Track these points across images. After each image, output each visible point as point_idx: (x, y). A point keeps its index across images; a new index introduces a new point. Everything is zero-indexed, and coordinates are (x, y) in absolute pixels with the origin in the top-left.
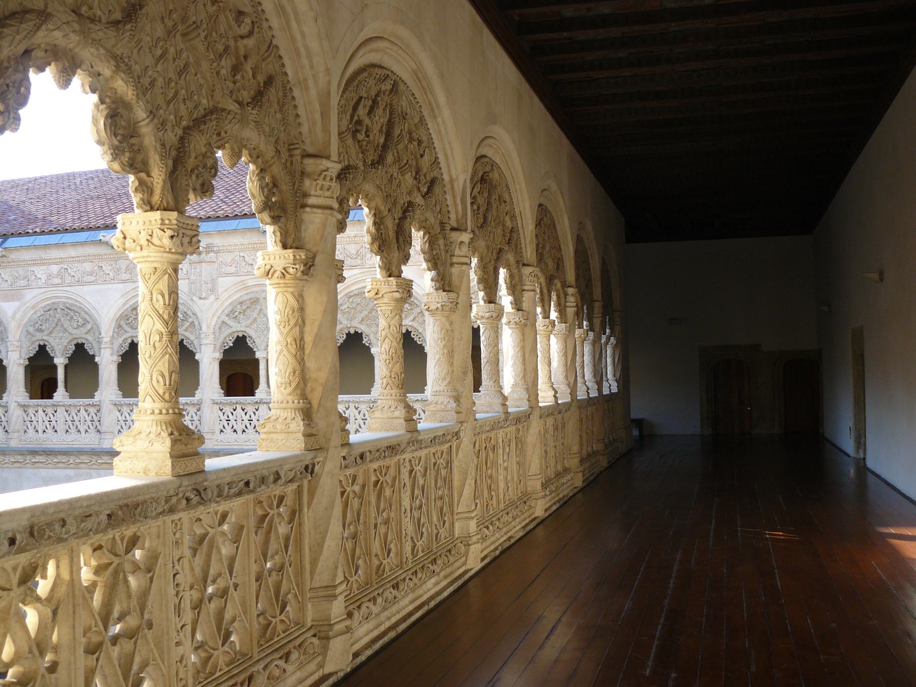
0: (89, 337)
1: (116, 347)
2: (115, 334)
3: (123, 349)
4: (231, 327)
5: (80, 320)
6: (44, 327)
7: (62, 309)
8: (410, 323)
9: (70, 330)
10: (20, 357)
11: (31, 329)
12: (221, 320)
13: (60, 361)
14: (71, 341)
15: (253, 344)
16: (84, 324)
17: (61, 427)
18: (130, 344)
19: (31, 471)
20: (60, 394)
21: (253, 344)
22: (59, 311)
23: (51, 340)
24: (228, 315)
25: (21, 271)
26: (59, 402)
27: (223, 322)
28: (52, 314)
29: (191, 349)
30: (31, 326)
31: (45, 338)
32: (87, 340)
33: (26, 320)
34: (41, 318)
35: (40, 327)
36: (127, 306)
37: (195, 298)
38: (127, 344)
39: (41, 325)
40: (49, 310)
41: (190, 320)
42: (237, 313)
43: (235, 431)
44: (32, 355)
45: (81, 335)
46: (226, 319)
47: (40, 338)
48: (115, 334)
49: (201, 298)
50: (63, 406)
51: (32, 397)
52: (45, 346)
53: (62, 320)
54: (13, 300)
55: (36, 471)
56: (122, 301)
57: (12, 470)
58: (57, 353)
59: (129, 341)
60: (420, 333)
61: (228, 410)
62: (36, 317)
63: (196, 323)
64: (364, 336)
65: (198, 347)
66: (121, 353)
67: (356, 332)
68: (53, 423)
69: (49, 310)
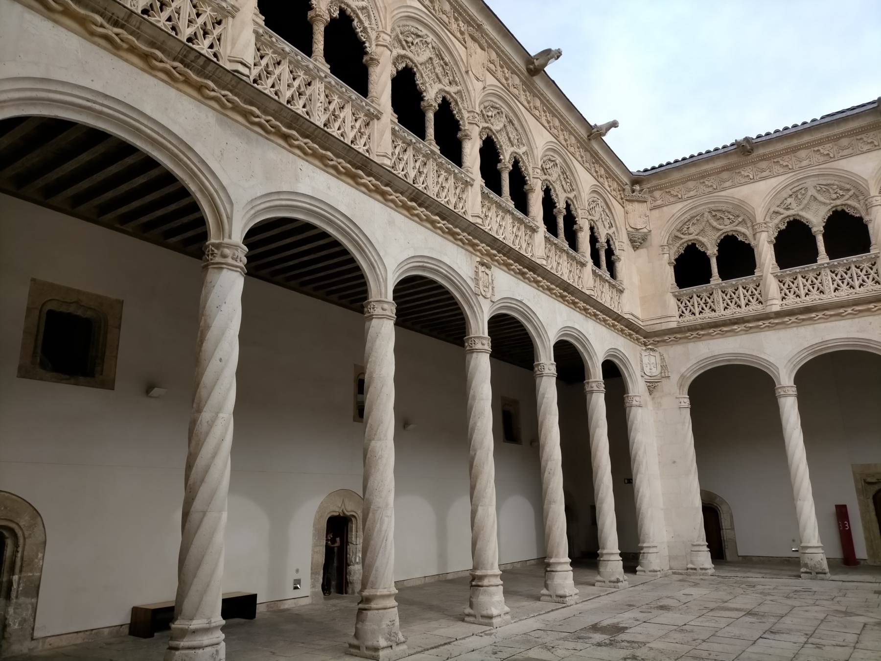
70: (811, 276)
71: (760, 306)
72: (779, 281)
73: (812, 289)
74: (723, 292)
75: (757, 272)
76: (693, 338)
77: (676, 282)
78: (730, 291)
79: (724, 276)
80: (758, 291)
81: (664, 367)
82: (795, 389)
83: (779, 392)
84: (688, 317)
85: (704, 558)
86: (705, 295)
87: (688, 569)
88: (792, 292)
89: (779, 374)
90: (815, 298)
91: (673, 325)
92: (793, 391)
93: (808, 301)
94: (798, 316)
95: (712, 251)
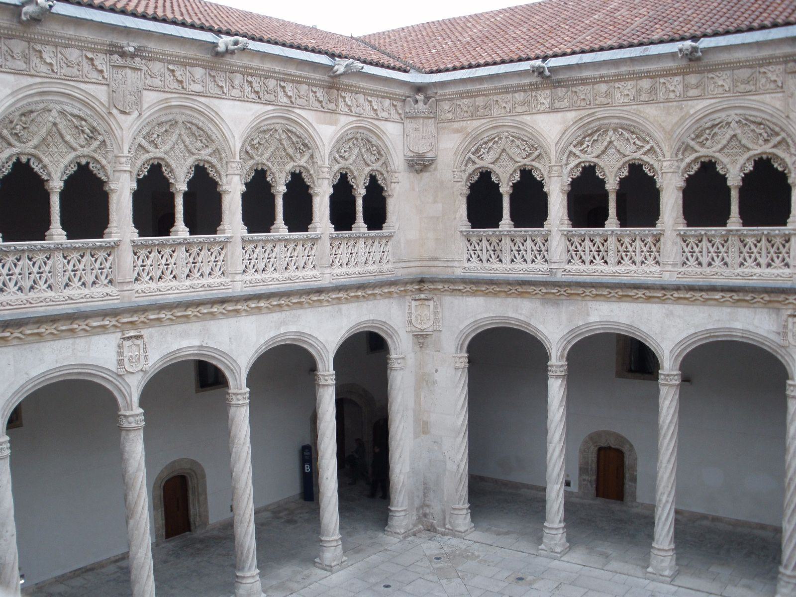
3: (4, 170)
4: (148, 152)
8: (305, 165)
12: (137, 142)
15: (170, 175)
18: (14, 164)
21: (170, 175)
24: (144, 138)
27: (140, 145)
29: (99, 176)
36: (13, 109)
37: (114, 111)
38: (10, 163)
41: (100, 138)
42: (155, 136)
43: (481, 260)
46: (144, 143)
49: (123, 112)
51: (575, 225)
60: (310, 175)
61: (576, 240)
63: (108, 143)
64: (268, 173)
65: (112, 174)
67: (262, 169)
68: (498, 252)
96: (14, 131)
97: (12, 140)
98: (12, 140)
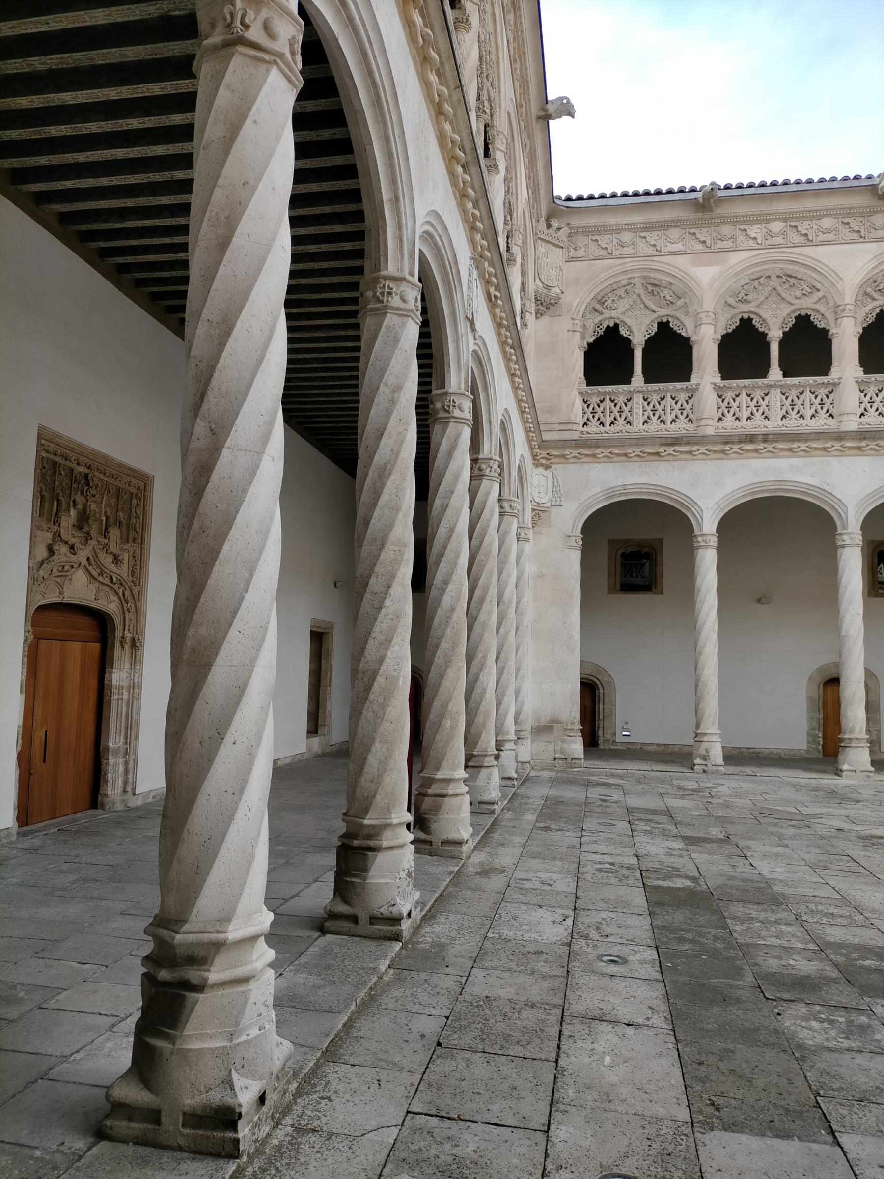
0: (821, 308)
1: (861, 316)
2: (859, 303)
3: (868, 320)
5: (807, 288)
6: (749, 298)
7: (778, 276)
9: (789, 299)
10: (715, 332)
11: (732, 301)
13: (775, 335)
14: (793, 312)
16: (811, 293)
17: (776, 413)
19: (736, 462)
20: (775, 373)
22: (774, 278)
23: (761, 313)
25: (726, 230)
26: (778, 381)
28: (762, 282)
30: (730, 296)
31: (752, 309)
32: (817, 311)
33: (724, 289)
34: (745, 287)
35: (745, 297)
36: (877, 271)
38: (874, 314)
39: (747, 295)
40: (757, 279)
44: (730, 331)
45: (806, 305)
47: (744, 309)
48: (859, 303)
50: (781, 386)
52: (750, 320)
53: (779, 288)
54: (710, 265)
55: (745, 462)
56: (873, 264)
57: (708, 462)
58: (771, 326)
59: (878, 311)
62: (739, 285)
66: (865, 325)
69: (757, 279)
70: (758, 394)
71: (691, 427)
72: (718, 395)
73: (755, 411)
74: (645, 400)
75: (694, 379)
76: (604, 457)
77: (585, 376)
78: (655, 398)
79: (649, 377)
80: (690, 405)
81: (556, 493)
82: (715, 539)
83: (698, 542)
84: (594, 428)
85: (577, 747)
86: (621, 400)
87: (555, 759)
88: (731, 413)
89: (702, 519)
90: (758, 425)
91: (575, 436)
92: (714, 541)
93: (748, 427)
94: (775, 444)
95: (638, 341)
96: (877, 289)
97: (875, 295)
98: (875, 295)
